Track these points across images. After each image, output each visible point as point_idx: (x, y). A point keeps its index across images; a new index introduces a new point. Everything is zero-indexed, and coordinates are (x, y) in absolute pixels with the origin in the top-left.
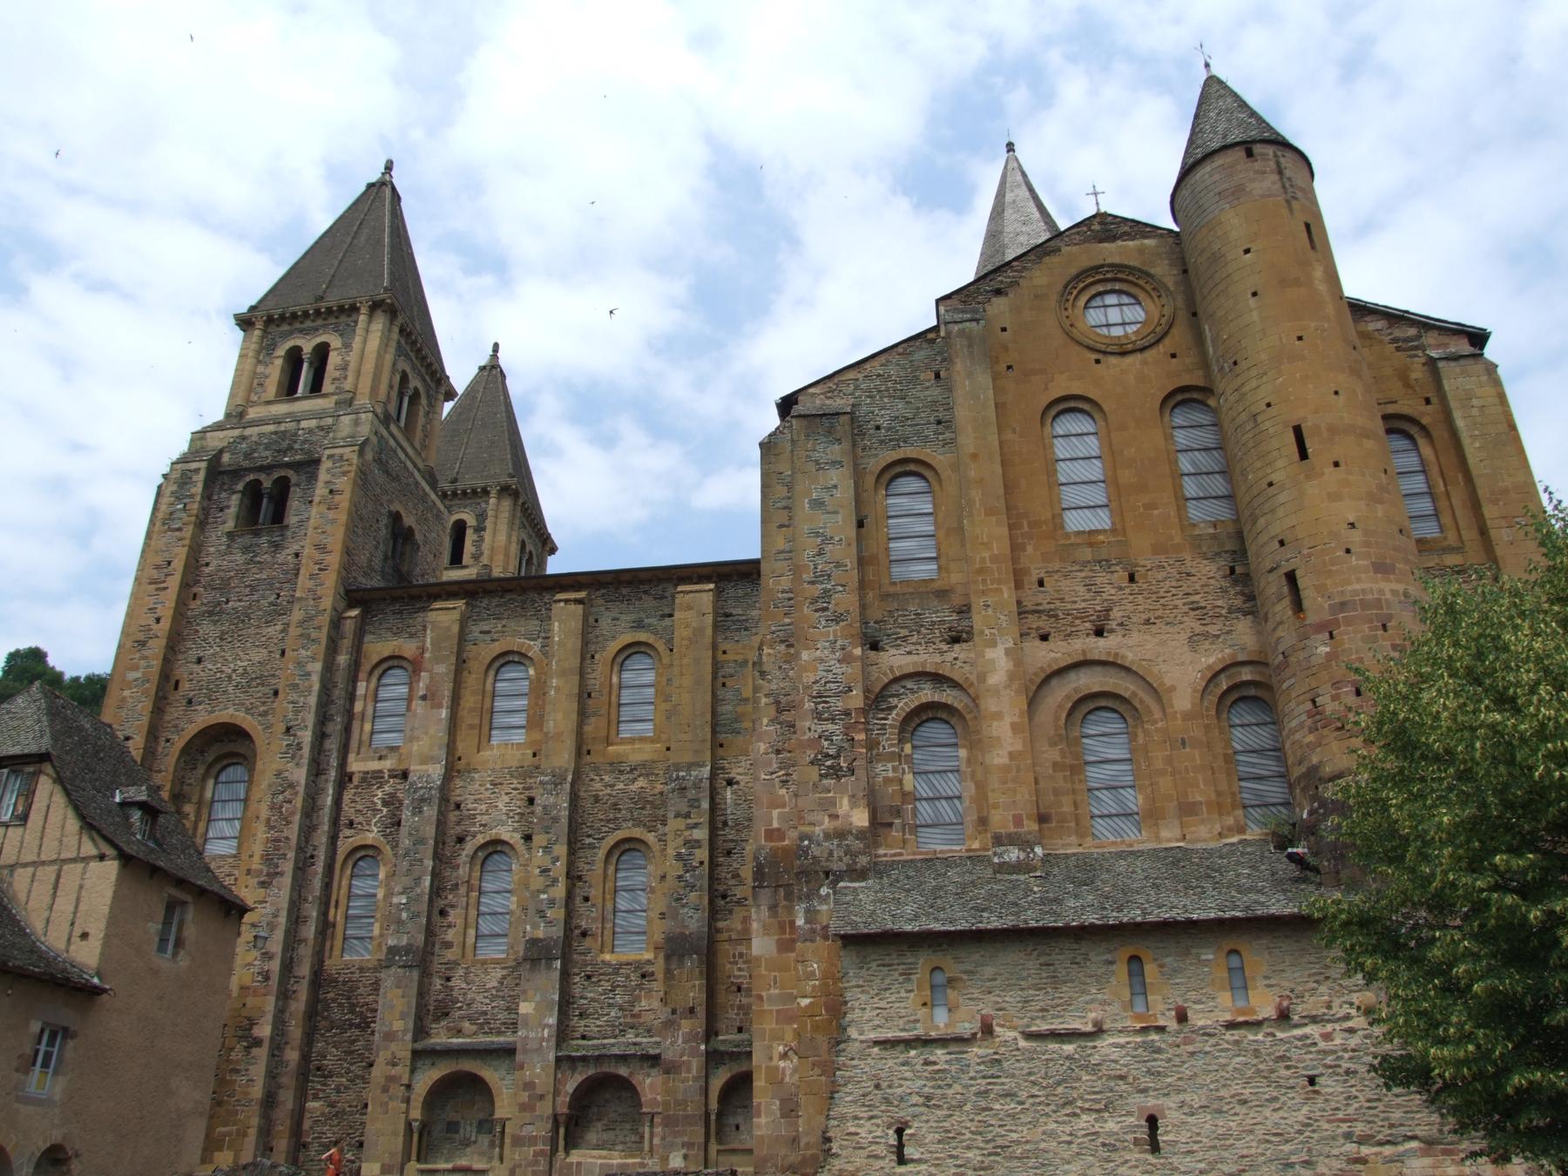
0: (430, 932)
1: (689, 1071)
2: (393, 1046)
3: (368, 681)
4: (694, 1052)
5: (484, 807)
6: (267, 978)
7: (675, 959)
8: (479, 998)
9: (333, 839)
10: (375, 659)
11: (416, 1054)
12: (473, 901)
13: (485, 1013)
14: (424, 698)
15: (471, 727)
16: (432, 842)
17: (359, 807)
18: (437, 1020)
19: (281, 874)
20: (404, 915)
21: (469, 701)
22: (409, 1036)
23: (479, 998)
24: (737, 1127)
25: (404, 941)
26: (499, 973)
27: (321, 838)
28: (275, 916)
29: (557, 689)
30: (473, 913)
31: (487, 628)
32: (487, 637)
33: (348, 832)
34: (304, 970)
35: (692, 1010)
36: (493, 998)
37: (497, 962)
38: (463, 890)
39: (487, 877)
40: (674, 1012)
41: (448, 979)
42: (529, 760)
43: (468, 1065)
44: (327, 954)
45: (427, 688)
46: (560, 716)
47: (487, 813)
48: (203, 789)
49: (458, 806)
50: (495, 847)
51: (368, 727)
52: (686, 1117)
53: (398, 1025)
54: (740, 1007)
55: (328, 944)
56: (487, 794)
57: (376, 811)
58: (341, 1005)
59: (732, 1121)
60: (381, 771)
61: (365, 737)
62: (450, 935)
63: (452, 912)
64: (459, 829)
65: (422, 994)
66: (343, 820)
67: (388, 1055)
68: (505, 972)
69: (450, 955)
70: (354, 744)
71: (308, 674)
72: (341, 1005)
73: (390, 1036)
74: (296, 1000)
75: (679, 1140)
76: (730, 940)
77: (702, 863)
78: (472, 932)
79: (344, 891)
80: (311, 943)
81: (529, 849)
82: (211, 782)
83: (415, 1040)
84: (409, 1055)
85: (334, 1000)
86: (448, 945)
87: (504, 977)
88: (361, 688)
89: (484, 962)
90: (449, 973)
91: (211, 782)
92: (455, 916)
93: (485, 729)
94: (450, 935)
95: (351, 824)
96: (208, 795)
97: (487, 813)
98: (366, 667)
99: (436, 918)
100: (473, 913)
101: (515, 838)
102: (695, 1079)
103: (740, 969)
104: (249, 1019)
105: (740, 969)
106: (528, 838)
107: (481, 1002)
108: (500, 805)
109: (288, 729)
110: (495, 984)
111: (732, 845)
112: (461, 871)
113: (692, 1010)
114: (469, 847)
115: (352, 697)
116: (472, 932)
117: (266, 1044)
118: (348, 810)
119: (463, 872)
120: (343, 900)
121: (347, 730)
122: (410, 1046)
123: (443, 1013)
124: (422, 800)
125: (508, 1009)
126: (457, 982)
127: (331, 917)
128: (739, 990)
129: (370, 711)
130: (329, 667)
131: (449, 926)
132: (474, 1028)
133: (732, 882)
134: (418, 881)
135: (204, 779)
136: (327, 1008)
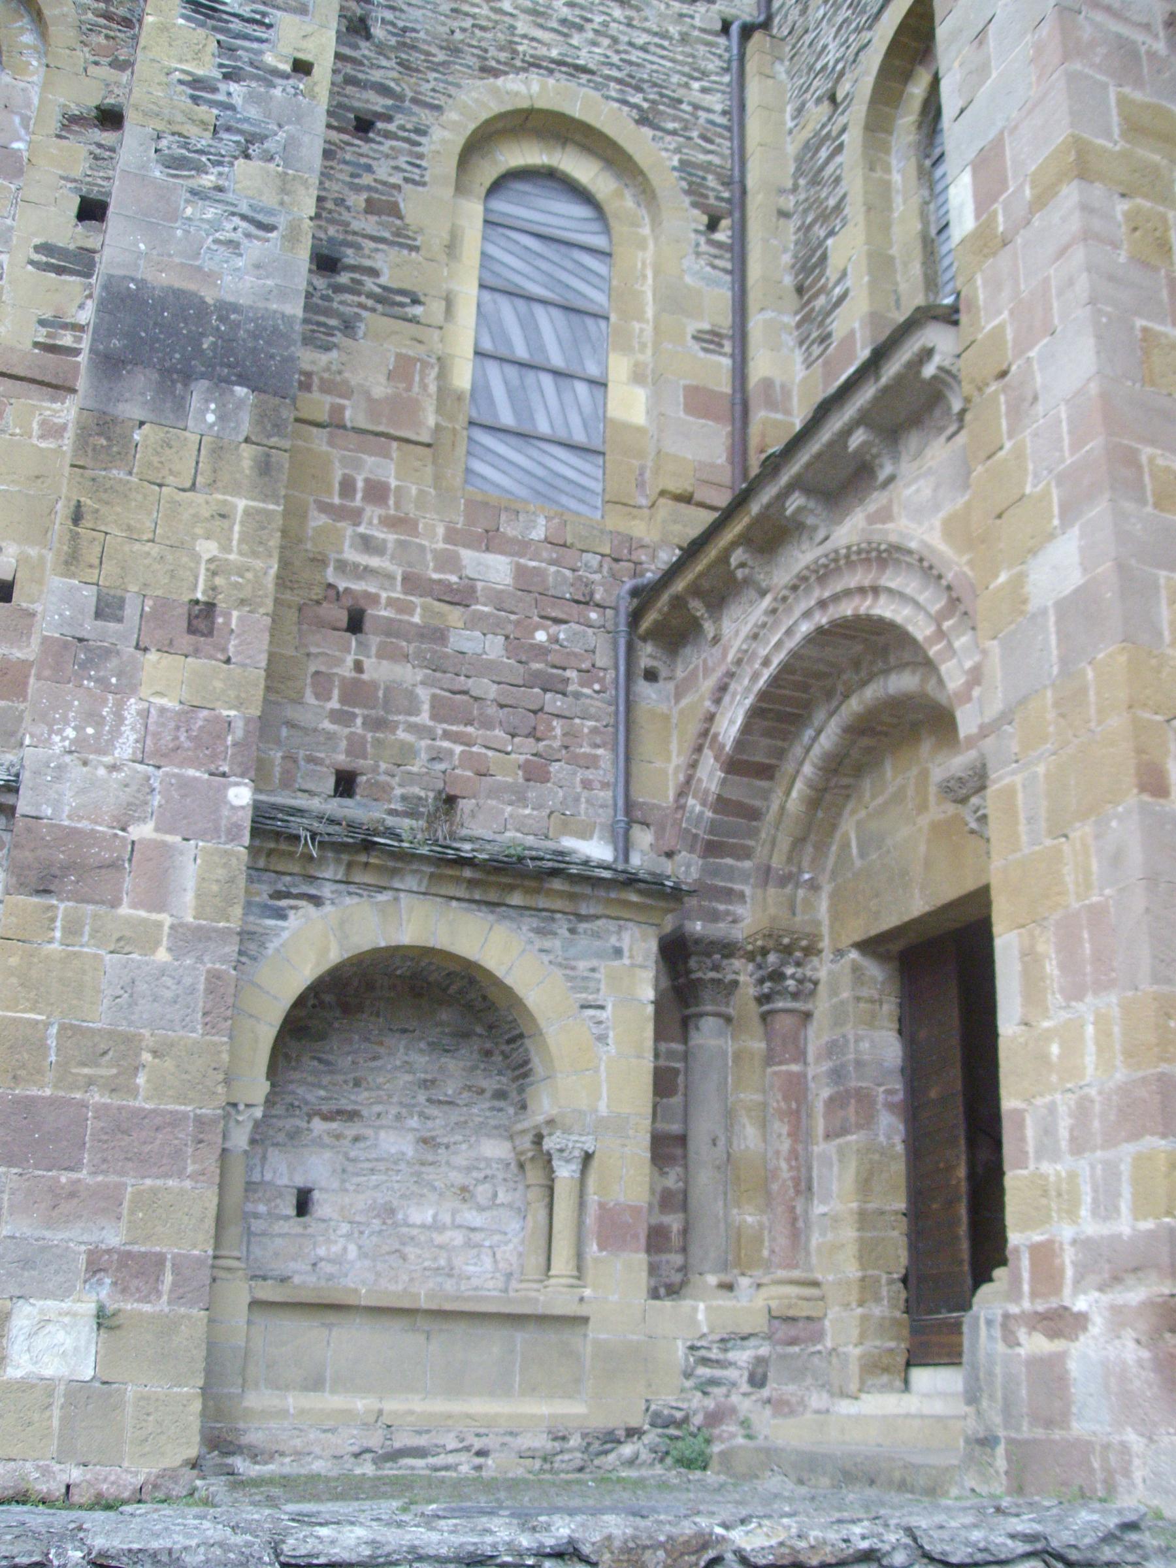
1: (157, 899)
4: (190, 814)
7: (142, 381)
24: (303, 1203)
35: (202, 618)
40: (107, 608)
52: (122, 1124)
54: (357, 692)
59: (284, 1171)
75: (77, 1238)
76: (335, 424)
77: (302, 67)
102: (188, 939)
103: (367, 544)
105: (367, 544)
111: (378, 103)
113: (202, 618)
128: (355, 624)
133: (369, 224)
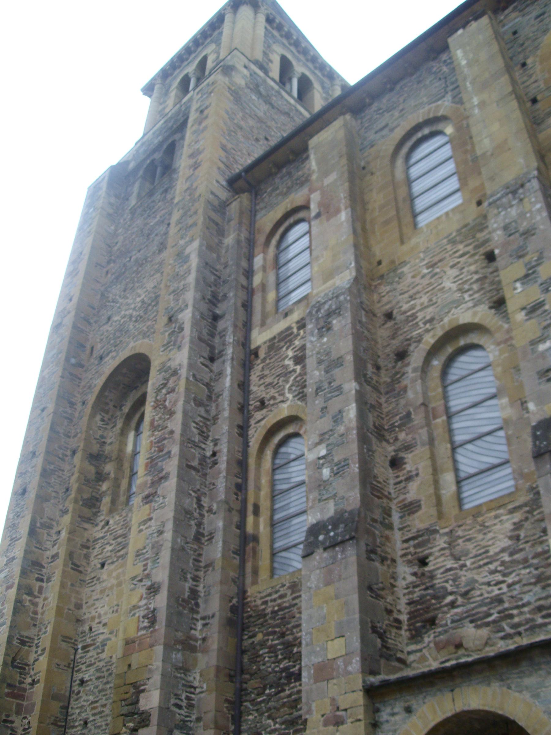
0: (368, 481)
2: (333, 688)
3: (264, 252)
5: (425, 299)
6: (153, 621)
8: (482, 576)
9: (243, 430)
10: (268, 227)
11: (375, 694)
12: (439, 431)
13: (499, 600)
14: (318, 215)
15: (387, 223)
16: (350, 358)
17: (268, 380)
18: (416, 635)
19: (165, 478)
20: (326, 472)
21: (377, 198)
22: (356, 664)
23: (482, 576)
25: (330, 510)
26: (507, 523)
27: (223, 429)
28: (160, 532)
29: (482, 105)
30: (443, 449)
31: (383, 124)
32: (384, 132)
33: (258, 415)
34: (213, 605)
36: (507, 569)
37: (497, 504)
38: (418, 419)
39: (452, 390)
41: (423, 562)
42: (473, 211)
43: (476, 697)
44: (249, 580)
45: (320, 205)
46: (495, 127)
47: (431, 303)
48: (123, 444)
49: (389, 316)
50: (457, 340)
51: (271, 296)
53: (335, 648)
55: (249, 566)
56: (426, 281)
57: (287, 374)
58: (273, 650)
60: (289, 328)
61: (270, 307)
62: (413, 492)
63: (409, 457)
64: (396, 343)
65: (372, 590)
66: (254, 403)
67: (328, 709)
68: (517, 517)
69: (419, 522)
70: (257, 318)
71: (188, 256)
72: (273, 650)
73: (325, 672)
74: (205, 651)
78: (448, 478)
79: (265, 492)
80: (218, 565)
81: (506, 317)
82: (131, 435)
83: (369, 668)
84: (359, 698)
85: (263, 644)
86: (411, 508)
87: (518, 526)
88: (258, 261)
89: (477, 512)
90: (423, 552)
91: (131, 435)
92: (416, 461)
93: (407, 219)
94: (413, 492)
95: (263, 404)
96: (129, 448)
97: (431, 303)
98: (261, 239)
99: (383, 471)
100: (443, 449)
101: (482, 314)
104: (134, 685)
106: (499, 304)
107: (484, 582)
108: (447, 284)
109: (170, 319)
110: (506, 543)
112: (410, 394)
114: (416, 358)
115: (249, 273)
116: (448, 478)
117: (154, 719)
118: (257, 389)
119: (414, 393)
120: (265, 504)
121: (247, 306)
122: (359, 684)
123: (424, 619)
124: (330, 314)
125: (539, 579)
126: (439, 562)
127: (250, 529)
129: (272, 278)
130: (211, 247)
131: (409, 479)
132: (484, 632)
134: (338, 418)
135: (123, 433)
136: (256, 658)
